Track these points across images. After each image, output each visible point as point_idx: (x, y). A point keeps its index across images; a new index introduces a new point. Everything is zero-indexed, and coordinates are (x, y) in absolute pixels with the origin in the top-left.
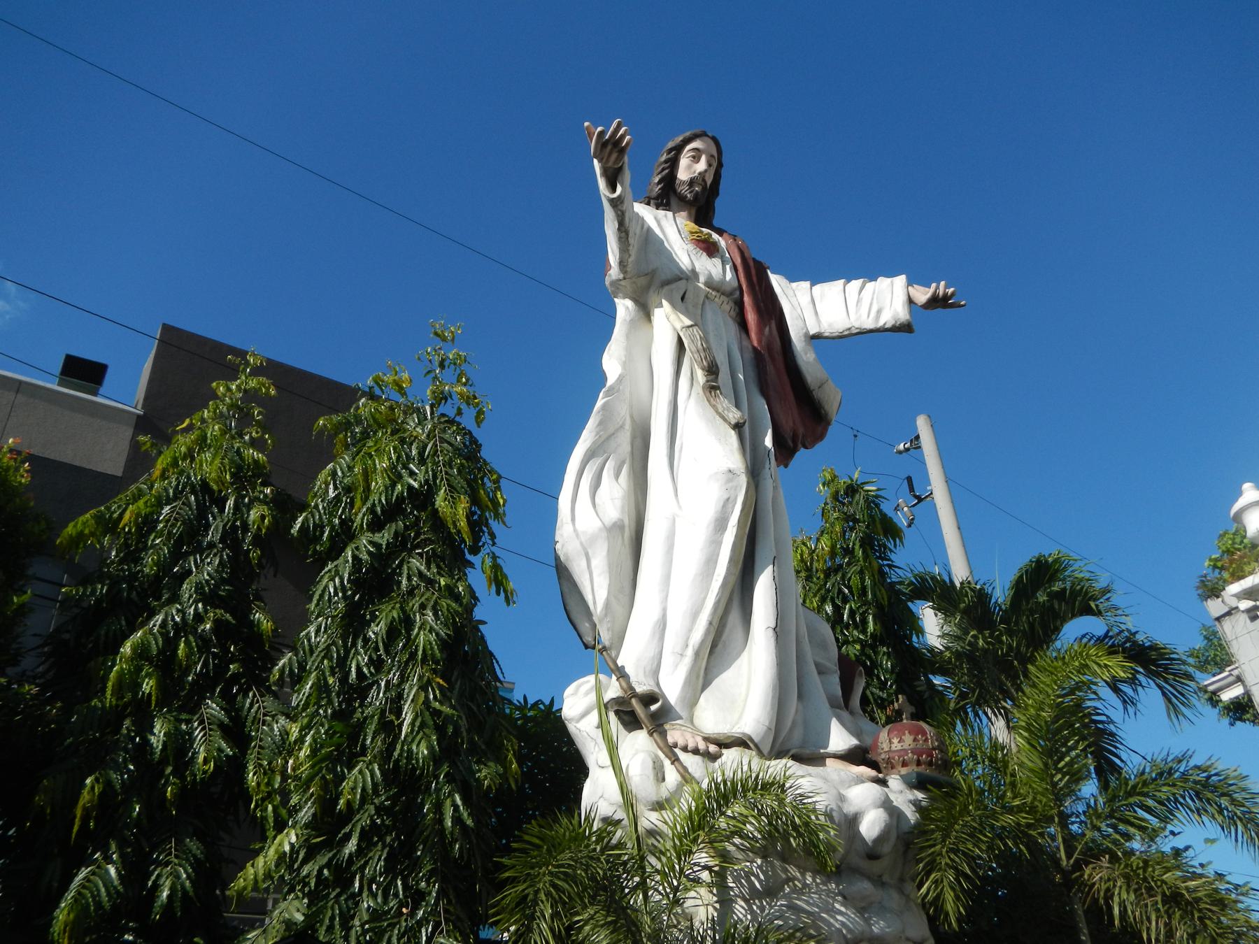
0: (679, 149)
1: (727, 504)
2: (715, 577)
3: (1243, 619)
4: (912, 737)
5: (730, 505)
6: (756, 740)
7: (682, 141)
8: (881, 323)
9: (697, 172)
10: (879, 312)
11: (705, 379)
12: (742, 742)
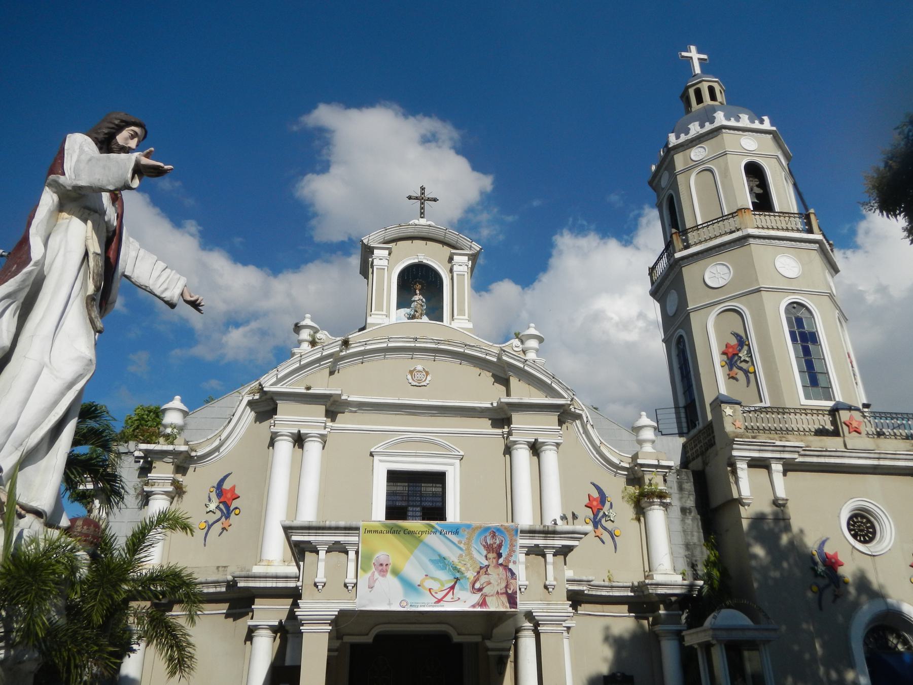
0: (128, 124)
1: (80, 377)
2: (53, 413)
3: (131, 459)
4: (94, 529)
5: (80, 378)
6: (48, 515)
7: (132, 122)
8: (163, 296)
9: (129, 145)
10: (166, 289)
11: (93, 293)
12: (38, 513)
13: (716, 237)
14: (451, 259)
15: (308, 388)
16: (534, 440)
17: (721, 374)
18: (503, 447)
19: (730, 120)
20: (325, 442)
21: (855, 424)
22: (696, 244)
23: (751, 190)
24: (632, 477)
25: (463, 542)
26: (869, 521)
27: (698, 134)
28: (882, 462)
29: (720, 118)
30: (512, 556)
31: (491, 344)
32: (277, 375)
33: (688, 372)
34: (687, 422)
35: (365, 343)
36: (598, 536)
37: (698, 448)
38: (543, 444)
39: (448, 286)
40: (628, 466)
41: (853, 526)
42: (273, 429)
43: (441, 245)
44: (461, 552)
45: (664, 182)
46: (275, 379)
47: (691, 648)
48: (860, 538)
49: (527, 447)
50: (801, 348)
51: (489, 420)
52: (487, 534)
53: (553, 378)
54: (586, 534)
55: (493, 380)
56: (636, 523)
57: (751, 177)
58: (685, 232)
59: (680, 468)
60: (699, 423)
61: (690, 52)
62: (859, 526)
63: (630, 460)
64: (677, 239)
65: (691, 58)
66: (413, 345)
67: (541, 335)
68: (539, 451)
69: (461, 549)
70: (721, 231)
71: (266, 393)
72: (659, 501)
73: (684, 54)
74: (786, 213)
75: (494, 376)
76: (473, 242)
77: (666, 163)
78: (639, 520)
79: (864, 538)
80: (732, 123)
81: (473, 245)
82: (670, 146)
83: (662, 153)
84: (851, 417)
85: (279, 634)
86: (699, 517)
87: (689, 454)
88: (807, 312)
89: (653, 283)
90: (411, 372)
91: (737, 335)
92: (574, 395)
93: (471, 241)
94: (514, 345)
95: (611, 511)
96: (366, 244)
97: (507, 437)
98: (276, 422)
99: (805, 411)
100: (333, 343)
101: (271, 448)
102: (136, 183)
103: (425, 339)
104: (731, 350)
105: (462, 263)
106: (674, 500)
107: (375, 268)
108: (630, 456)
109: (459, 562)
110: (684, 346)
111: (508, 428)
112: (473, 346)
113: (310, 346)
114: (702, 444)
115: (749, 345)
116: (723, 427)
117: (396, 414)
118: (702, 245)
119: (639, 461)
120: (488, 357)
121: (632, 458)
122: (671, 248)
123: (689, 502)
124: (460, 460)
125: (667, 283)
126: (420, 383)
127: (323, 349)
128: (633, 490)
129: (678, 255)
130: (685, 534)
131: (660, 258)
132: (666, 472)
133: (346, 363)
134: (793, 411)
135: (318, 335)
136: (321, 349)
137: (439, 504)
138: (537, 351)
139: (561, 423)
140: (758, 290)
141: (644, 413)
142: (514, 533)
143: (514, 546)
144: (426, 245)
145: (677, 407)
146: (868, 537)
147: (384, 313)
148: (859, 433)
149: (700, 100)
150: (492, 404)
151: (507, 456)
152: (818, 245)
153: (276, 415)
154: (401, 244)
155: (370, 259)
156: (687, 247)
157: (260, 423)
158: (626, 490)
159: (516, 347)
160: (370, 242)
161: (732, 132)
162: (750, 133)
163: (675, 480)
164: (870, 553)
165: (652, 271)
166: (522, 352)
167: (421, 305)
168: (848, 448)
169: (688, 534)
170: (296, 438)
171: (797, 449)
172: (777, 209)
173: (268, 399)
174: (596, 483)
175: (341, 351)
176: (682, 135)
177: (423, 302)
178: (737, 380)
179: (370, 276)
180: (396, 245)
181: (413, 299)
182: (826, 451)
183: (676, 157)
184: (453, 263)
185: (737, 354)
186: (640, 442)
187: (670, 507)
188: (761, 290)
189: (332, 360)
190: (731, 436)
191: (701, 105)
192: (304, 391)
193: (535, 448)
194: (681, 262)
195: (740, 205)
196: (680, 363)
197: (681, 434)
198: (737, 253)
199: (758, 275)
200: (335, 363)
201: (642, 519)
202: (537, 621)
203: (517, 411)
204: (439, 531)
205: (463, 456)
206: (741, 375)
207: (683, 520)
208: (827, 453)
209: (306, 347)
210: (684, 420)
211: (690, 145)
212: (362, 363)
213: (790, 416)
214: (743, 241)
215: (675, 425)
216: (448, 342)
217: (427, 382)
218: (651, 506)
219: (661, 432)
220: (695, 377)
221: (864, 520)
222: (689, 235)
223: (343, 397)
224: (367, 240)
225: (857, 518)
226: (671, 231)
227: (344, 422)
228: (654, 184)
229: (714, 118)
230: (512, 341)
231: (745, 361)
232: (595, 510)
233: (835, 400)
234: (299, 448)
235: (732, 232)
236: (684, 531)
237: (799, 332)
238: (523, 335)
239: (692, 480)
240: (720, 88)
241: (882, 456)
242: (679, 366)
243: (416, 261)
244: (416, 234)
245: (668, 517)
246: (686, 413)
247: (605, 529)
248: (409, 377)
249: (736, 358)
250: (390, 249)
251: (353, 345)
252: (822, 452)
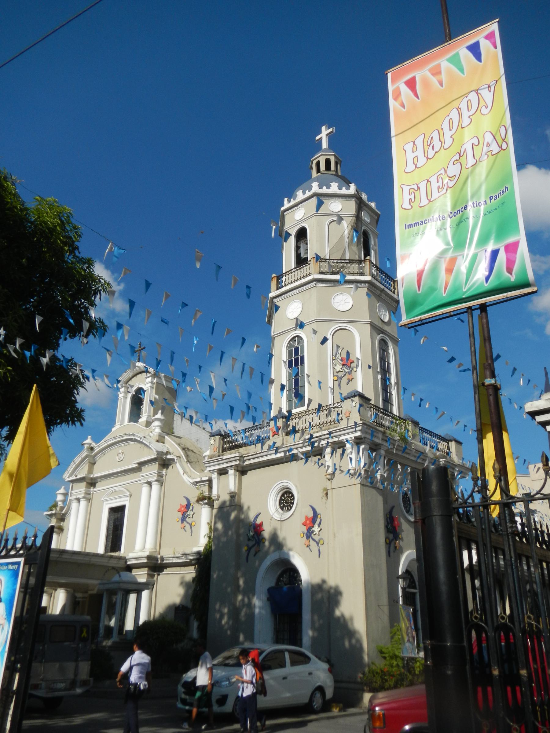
15: (76, 476)
20: (90, 500)
32: (69, 472)
36: (182, 528)
48: (286, 508)
72: (202, 502)
95: (191, 511)
112: (131, 434)
117: (113, 478)
124: (130, 497)
133: (98, 457)
152: (314, 282)
154: (133, 379)
161: (290, 211)
171: (236, 458)
174: (187, 496)
175: (92, 453)
182: (257, 454)
188: (275, 337)
203: (143, 466)
216: (124, 435)
221: (291, 495)
225: (287, 495)
227: (99, 487)
243: (137, 387)
244: (136, 373)
247: (188, 523)
248: (117, 457)
251: (95, 449)
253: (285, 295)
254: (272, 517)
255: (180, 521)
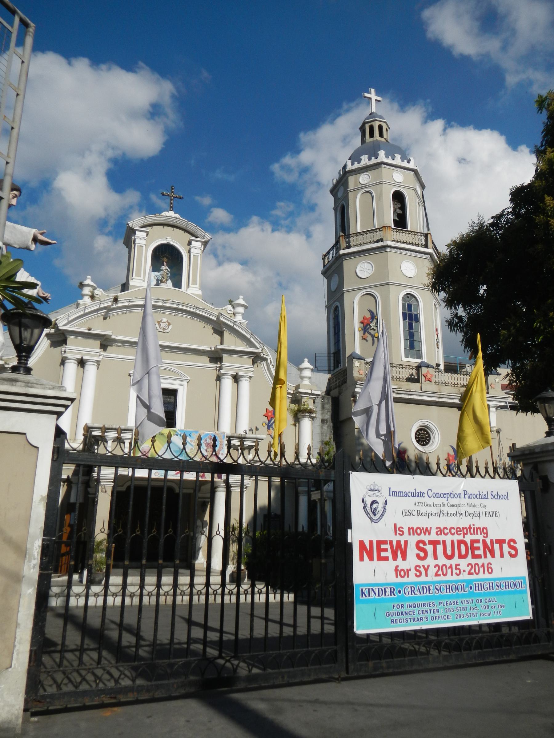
13: (367, 243)
14: (189, 243)
15: (90, 329)
16: (235, 374)
17: (358, 335)
18: (216, 376)
19: (389, 157)
20: (99, 365)
21: (429, 376)
22: (354, 246)
23: (395, 211)
24: (294, 399)
25: (193, 441)
26: (428, 433)
27: (366, 165)
28: (441, 400)
29: (382, 156)
30: (221, 451)
31: (213, 307)
32: (68, 318)
33: (339, 332)
34: (334, 363)
35: (128, 300)
37: (337, 382)
38: (241, 376)
39: (187, 262)
40: (292, 392)
41: (419, 435)
42: (65, 355)
43: (183, 232)
44: (192, 447)
45: (340, 194)
46: (66, 321)
47: (314, 501)
48: (421, 442)
49: (231, 377)
50: (408, 324)
51: (208, 357)
52: (207, 437)
53: (252, 335)
54: (262, 440)
55: (213, 331)
56: (293, 427)
57: (396, 201)
58: (348, 236)
59: (325, 395)
60: (340, 365)
61: (371, 94)
62: (422, 435)
63: (294, 389)
64: (343, 241)
65: (371, 99)
66: (161, 304)
67: (247, 305)
68: (238, 380)
69: (192, 445)
70: (371, 240)
71: (60, 330)
72: (309, 415)
73: (366, 95)
74: (413, 232)
75: (213, 329)
76: (206, 233)
77: (343, 181)
78: (295, 425)
79: (423, 443)
80: (389, 161)
81: (205, 235)
82: (347, 170)
83: (341, 172)
84: (428, 371)
85: (66, 484)
86: (332, 424)
87: (332, 385)
88: (415, 300)
89: (324, 266)
90: (159, 322)
91: (371, 312)
92: (264, 347)
93: (204, 232)
94: (228, 309)
96: (131, 226)
97: (219, 370)
98: (66, 350)
99: (402, 366)
100: (107, 300)
101: (62, 366)
102: (33, 247)
103: (169, 301)
104: (366, 321)
105: (197, 245)
106: (319, 416)
107: (136, 245)
108: (295, 386)
109: (191, 453)
110: (338, 313)
111: (220, 364)
112: (202, 309)
113: (90, 299)
114: (340, 380)
115: (377, 319)
116: (352, 374)
118: (358, 247)
119: (300, 390)
120: (211, 317)
121: (296, 387)
122: (338, 246)
123: (327, 416)
125: (333, 268)
126: (164, 330)
127: (101, 304)
128: (294, 407)
129: (341, 252)
130: (322, 435)
131: (331, 250)
132: (315, 398)
134: (395, 366)
135: (96, 292)
136: (99, 303)
137: (172, 410)
138: (243, 314)
139: (254, 363)
140: (388, 284)
141: (306, 360)
142: (222, 437)
143: (223, 445)
144: (173, 230)
145: (329, 353)
146: (426, 442)
147: (142, 278)
148: (431, 382)
149: (372, 135)
150: (211, 348)
151: (218, 382)
152: (429, 256)
153: (66, 344)
154: (155, 228)
155: (133, 238)
156: (349, 247)
157: (54, 348)
158: (290, 406)
159: (229, 310)
160: (133, 225)
161: (388, 167)
162: (400, 169)
163: (320, 402)
164: (424, 452)
165: (325, 257)
166: (233, 314)
167: (167, 273)
168: (423, 390)
169: (323, 435)
170: (79, 361)
172: (409, 229)
173: (60, 333)
175: (112, 305)
176: (356, 163)
177: (168, 271)
178: (367, 341)
179: (133, 250)
180: (152, 228)
181: (161, 269)
182: (410, 391)
183: (350, 178)
184: (191, 247)
185: (369, 324)
186: (302, 378)
187: (316, 418)
189: (106, 311)
190: (356, 379)
191: (372, 139)
192: (87, 331)
193: (236, 379)
194: (343, 257)
195: (386, 223)
196: (334, 323)
197: (329, 371)
198: (378, 256)
199: (389, 274)
200: (107, 313)
201: (297, 425)
202: (231, 485)
204: (179, 434)
205: (189, 380)
206: (369, 338)
207: (322, 427)
208: (410, 393)
209: (87, 300)
210: (332, 361)
211: (360, 171)
212: (126, 313)
213: (393, 369)
214: (383, 248)
215: (327, 365)
216: (185, 304)
217: (169, 330)
218: (304, 417)
219: (317, 368)
220: (342, 335)
221: (426, 432)
222: (351, 239)
223: (113, 337)
224: (132, 224)
225: (421, 431)
226: (340, 234)
227: (112, 353)
228: (334, 193)
229: (378, 154)
230: (227, 306)
231: (373, 329)
232: (269, 418)
233: (422, 359)
234: (81, 367)
235: (378, 241)
236: (322, 433)
237: (408, 313)
238: (235, 304)
239: (331, 403)
240: (386, 127)
241: (441, 396)
242: (333, 326)
243: (165, 242)
244: (167, 222)
245: (313, 425)
246: (334, 357)
248: (157, 325)
249: (369, 326)
250: (148, 233)
251: (120, 302)
252: (408, 392)
253: (400, 250)
254: (416, 448)
255: (266, 427)
